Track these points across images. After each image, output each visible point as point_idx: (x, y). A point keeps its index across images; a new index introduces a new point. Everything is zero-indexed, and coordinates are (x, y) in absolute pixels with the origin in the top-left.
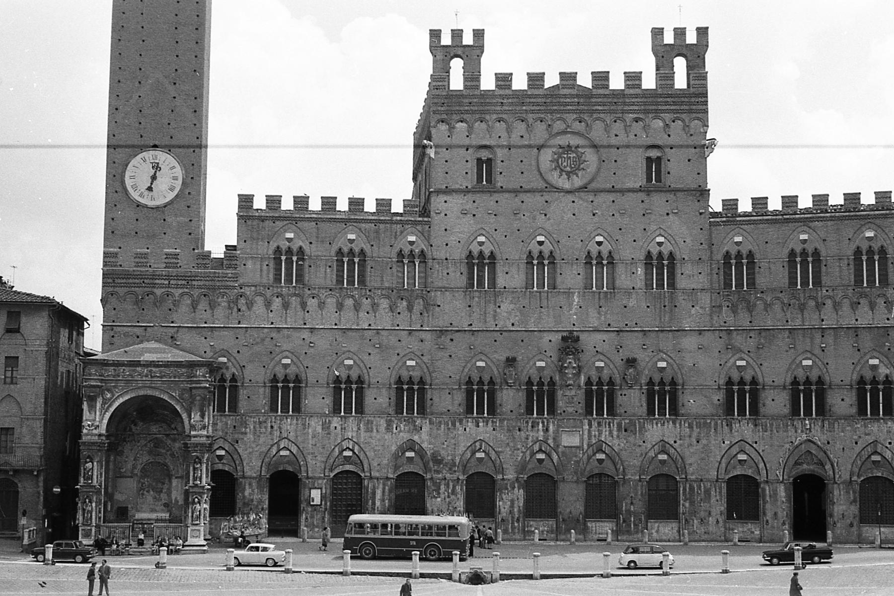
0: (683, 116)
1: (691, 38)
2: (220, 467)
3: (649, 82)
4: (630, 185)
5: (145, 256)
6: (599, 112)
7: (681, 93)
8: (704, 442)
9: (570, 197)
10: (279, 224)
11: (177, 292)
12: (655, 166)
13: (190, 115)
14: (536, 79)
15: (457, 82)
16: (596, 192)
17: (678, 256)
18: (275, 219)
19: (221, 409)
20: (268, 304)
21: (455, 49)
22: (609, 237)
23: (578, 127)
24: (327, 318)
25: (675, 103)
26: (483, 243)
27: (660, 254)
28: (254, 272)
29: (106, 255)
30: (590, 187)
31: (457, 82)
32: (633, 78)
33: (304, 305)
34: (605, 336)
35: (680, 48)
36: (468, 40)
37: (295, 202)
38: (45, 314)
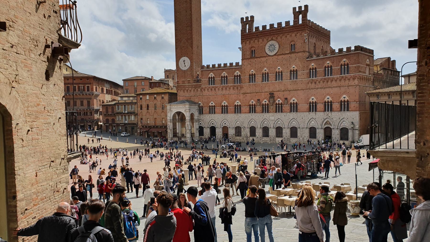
1: (303, 9)
3: (292, 24)
4: (287, 52)
5: (184, 81)
6: (279, 34)
9: (272, 57)
11: (190, 89)
12: (293, 47)
14: (264, 27)
17: (298, 70)
19: (200, 113)
20: (208, 90)
21: (247, 22)
24: (220, 92)
25: (298, 28)
26: (253, 71)
27: (294, 70)
30: (277, 54)
32: (287, 23)
33: (215, 89)
34: (280, 92)
35: (300, 12)
38: (168, 95)
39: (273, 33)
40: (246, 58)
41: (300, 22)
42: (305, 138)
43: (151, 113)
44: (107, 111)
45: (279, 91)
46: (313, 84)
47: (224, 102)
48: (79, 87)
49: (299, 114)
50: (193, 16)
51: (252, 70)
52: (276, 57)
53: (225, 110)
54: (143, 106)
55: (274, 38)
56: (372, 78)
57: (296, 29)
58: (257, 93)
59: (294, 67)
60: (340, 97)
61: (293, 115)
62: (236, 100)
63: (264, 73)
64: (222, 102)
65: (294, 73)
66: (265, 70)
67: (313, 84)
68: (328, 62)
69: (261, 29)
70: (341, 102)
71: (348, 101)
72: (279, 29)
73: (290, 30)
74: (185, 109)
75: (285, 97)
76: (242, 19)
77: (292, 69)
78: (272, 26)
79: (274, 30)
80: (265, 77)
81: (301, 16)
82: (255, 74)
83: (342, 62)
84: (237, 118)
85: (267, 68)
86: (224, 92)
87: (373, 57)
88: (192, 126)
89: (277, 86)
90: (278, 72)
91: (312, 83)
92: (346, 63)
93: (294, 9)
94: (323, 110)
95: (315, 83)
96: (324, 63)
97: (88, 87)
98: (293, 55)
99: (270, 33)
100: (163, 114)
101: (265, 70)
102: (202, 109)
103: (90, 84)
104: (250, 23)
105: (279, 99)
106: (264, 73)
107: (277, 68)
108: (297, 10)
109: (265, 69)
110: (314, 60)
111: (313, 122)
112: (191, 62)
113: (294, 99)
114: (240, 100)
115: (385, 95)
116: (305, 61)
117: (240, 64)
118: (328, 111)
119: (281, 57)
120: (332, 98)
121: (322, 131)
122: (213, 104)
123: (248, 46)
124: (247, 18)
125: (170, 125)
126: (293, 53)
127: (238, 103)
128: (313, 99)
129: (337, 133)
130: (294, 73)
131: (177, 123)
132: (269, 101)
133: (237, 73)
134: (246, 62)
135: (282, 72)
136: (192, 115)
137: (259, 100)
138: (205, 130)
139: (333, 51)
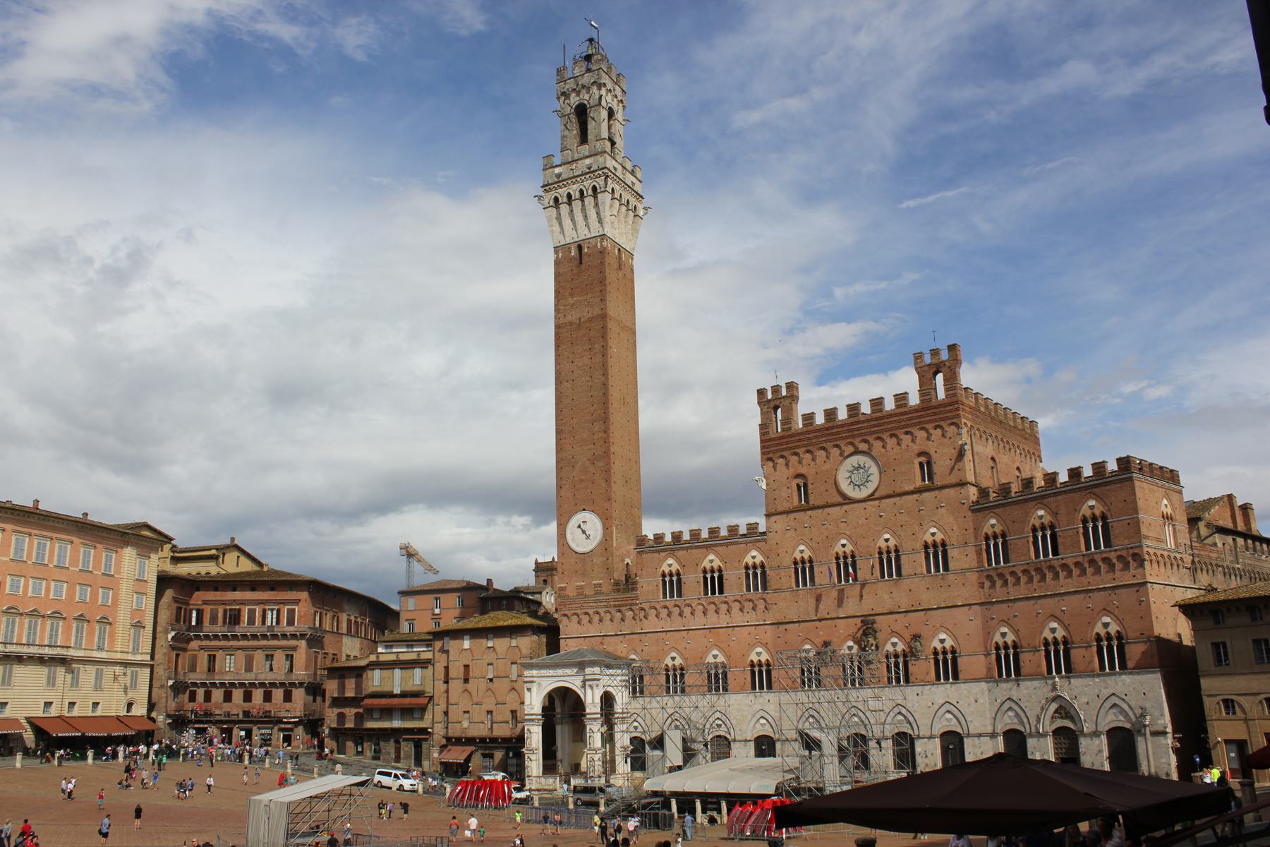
0: (942, 423)
1: (944, 356)
3: (914, 400)
5: (581, 587)
7: (942, 405)
9: (863, 505)
10: (663, 554)
12: (927, 467)
13: (603, 484)
16: (880, 499)
17: (947, 541)
18: (659, 552)
19: (634, 691)
22: (894, 533)
23: (863, 447)
24: (699, 621)
25: (935, 414)
26: (802, 551)
32: (901, 398)
36: (784, 393)
40: (780, 509)
41: (941, 394)
43: (474, 693)
44: (342, 688)
45: (891, 613)
47: (715, 652)
48: (264, 611)
49: (963, 687)
50: (611, 390)
51: (802, 547)
52: (876, 503)
54: (452, 673)
55: (863, 447)
56: (1188, 559)
57: (928, 415)
58: (820, 620)
59: (933, 533)
60: (1091, 624)
61: (944, 692)
62: (752, 646)
63: (841, 554)
64: (706, 653)
66: (844, 546)
68: (1041, 513)
69: (820, 420)
70: (1098, 638)
71: (1119, 636)
72: (877, 419)
73: (912, 419)
75: (915, 630)
76: (761, 393)
77: (930, 540)
78: (853, 409)
79: (863, 422)
80: (847, 565)
81: (940, 378)
82: (811, 561)
85: (849, 538)
86: (712, 620)
87: (1180, 493)
88: (609, 738)
89: (886, 596)
92: (1097, 512)
97: (291, 612)
98: (927, 496)
99: (849, 431)
100: (513, 695)
101: (843, 545)
103: (297, 602)
104: (787, 402)
105: (895, 640)
106: (841, 554)
107: (880, 537)
108: (928, 359)
109: (844, 541)
112: (606, 528)
113: (943, 636)
114: (765, 646)
115: (1229, 610)
116: (970, 513)
117: (762, 529)
119: (888, 501)
120: (1066, 628)
122: (678, 661)
123: (783, 472)
124: (776, 389)
125: (535, 736)
126: (928, 489)
127: (760, 654)
130: (938, 553)
131: (558, 728)
133: (754, 556)
134: (780, 523)
135: (897, 551)
136: (607, 700)
137: (826, 644)
139: (1051, 478)
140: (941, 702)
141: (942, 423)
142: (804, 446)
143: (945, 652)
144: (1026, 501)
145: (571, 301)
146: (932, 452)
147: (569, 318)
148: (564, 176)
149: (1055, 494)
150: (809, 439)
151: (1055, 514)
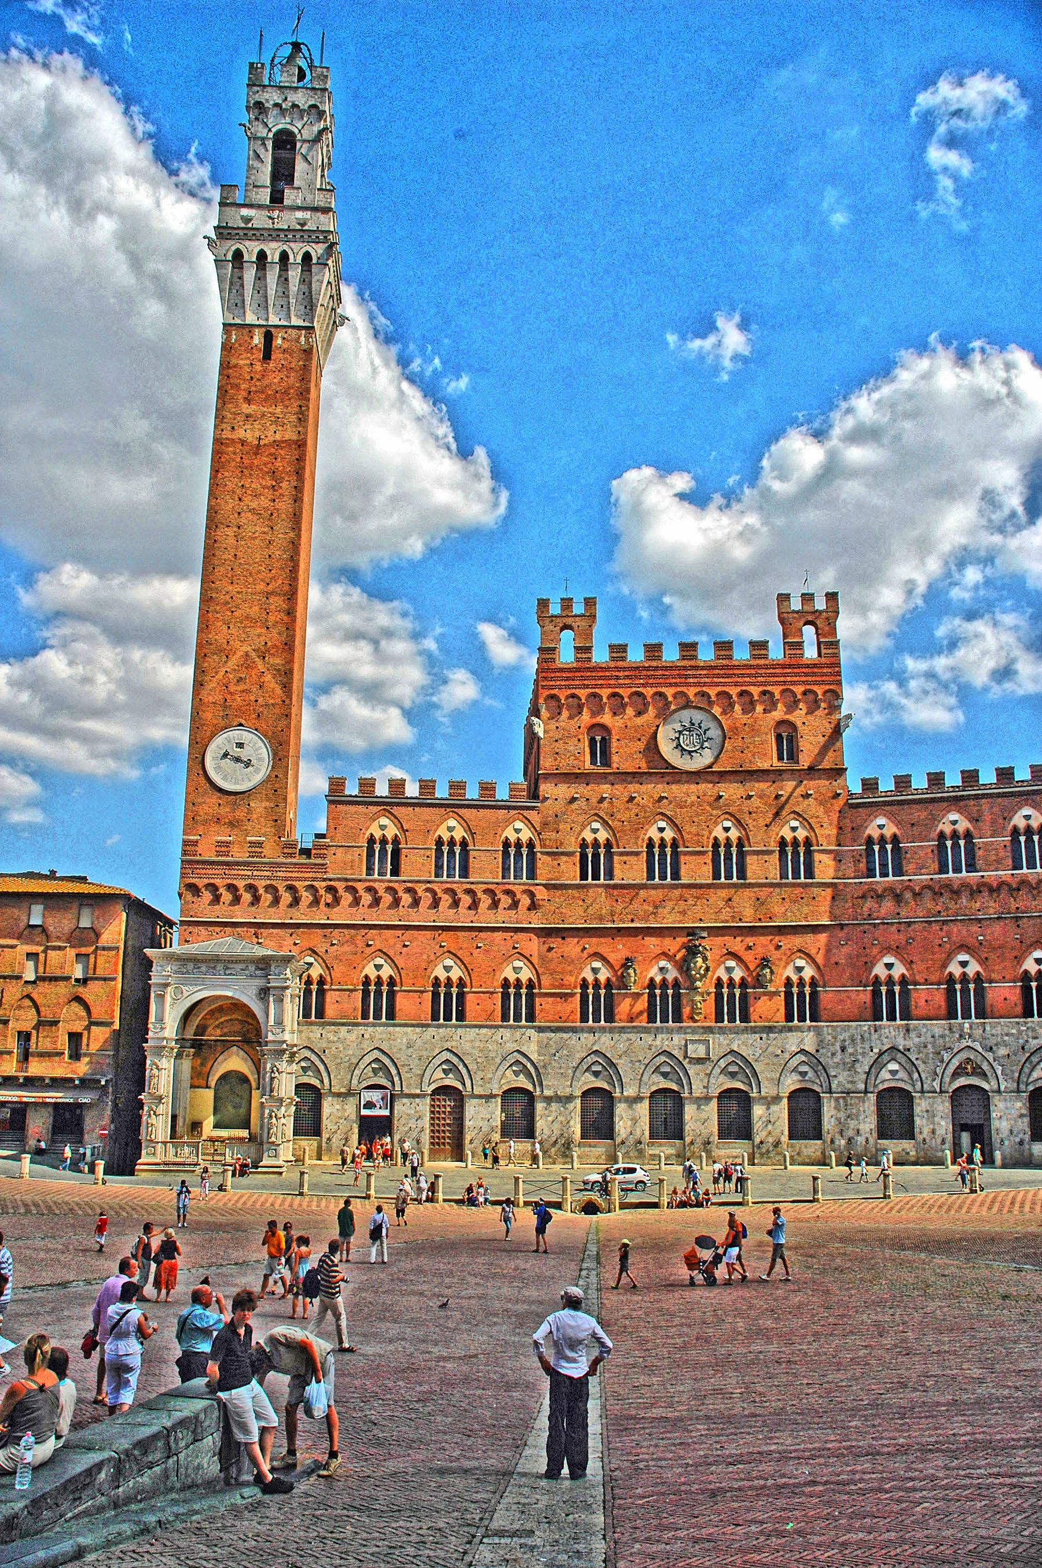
0: (815, 688)
2: (305, 1080)
3: (776, 653)
5: (227, 844)
8: (850, 1050)
10: (374, 809)
13: (278, 691)
15: (566, 655)
19: (307, 1015)
25: (806, 675)
28: (346, 862)
29: (186, 843)
31: (566, 655)
36: (578, 609)
37: (391, 786)
39: (695, 676)
42: (860, 1140)
46: (888, 905)
53: (449, 1004)
65: (796, 854)
67: (888, 905)
74: (260, 982)
83: (1018, 821)
84: (511, 1046)
90: (723, 842)
91: (879, 897)
93: (783, 598)
94: (943, 1011)
95: (898, 898)
96: (934, 819)
99: (680, 676)
102: (321, 993)
110: (885, 803)
111: (893, 1066)
118: (966, 1016)
121: (943, 1106)
128: (889, 966)
129: (1015, 1113)
132: (684, 966)
138: (329, 1107)
140: (794, 1049)
141: (815, 688)
142: (609, 686)
143: (801, 983)
144: (933, 800)
145: (246, 409)
146: (799, 724)
147: (241, 434)
148: (256, 224)
149: (977, 797)
150: (618, 678)
151: (975, 820)
